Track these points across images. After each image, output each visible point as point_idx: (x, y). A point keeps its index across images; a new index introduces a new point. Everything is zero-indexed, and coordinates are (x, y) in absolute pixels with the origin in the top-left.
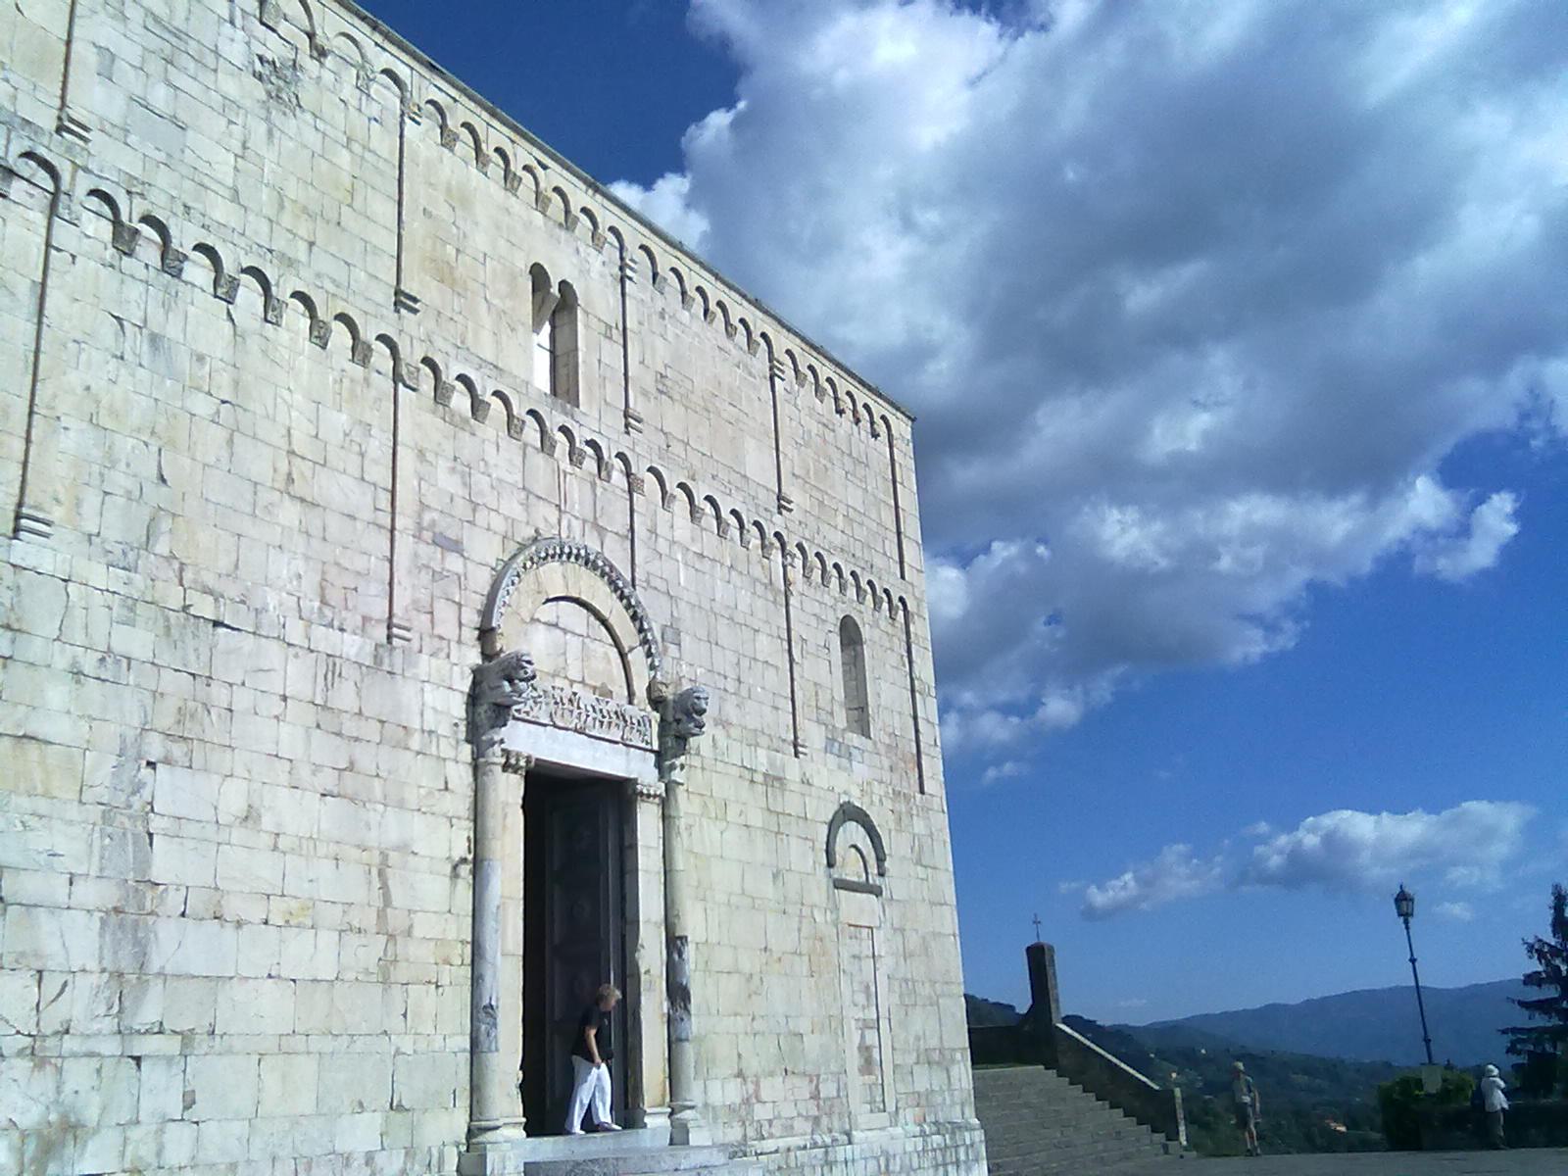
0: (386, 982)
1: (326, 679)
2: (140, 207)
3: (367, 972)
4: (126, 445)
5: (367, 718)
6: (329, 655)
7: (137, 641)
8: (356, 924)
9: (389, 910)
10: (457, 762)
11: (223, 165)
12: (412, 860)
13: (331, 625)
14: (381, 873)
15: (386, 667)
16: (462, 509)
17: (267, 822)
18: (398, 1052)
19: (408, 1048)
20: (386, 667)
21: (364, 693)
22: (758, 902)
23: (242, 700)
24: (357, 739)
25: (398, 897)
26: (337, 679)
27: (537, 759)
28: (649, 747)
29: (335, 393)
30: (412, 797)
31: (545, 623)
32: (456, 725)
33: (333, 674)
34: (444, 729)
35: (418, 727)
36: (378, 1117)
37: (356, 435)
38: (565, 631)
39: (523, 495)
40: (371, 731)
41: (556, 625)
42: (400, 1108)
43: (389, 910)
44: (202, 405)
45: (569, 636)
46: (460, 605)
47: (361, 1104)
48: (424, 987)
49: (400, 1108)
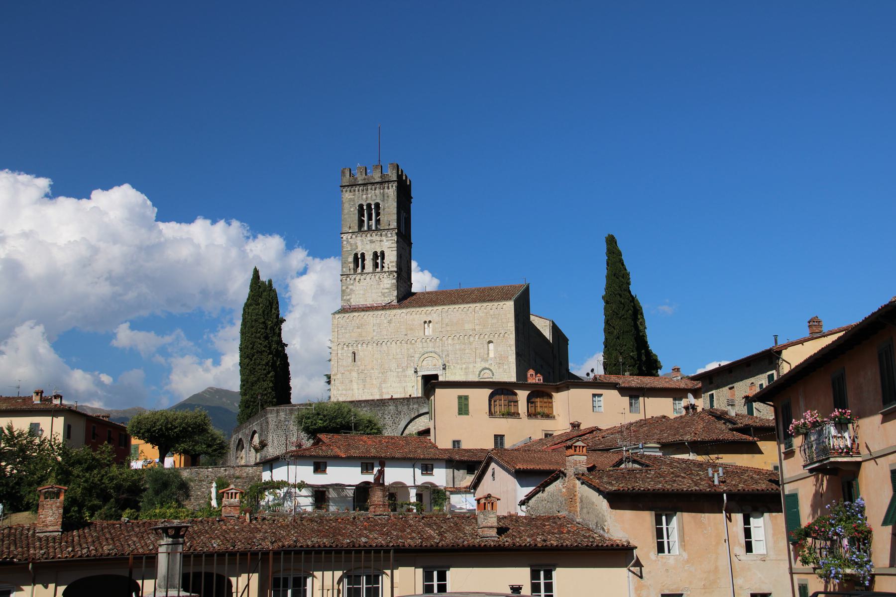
4: (379, 361)
7: (380, 375)
11: (385, 333)
23: (389, 377)
25: (406, 390)
44: (385, 355)
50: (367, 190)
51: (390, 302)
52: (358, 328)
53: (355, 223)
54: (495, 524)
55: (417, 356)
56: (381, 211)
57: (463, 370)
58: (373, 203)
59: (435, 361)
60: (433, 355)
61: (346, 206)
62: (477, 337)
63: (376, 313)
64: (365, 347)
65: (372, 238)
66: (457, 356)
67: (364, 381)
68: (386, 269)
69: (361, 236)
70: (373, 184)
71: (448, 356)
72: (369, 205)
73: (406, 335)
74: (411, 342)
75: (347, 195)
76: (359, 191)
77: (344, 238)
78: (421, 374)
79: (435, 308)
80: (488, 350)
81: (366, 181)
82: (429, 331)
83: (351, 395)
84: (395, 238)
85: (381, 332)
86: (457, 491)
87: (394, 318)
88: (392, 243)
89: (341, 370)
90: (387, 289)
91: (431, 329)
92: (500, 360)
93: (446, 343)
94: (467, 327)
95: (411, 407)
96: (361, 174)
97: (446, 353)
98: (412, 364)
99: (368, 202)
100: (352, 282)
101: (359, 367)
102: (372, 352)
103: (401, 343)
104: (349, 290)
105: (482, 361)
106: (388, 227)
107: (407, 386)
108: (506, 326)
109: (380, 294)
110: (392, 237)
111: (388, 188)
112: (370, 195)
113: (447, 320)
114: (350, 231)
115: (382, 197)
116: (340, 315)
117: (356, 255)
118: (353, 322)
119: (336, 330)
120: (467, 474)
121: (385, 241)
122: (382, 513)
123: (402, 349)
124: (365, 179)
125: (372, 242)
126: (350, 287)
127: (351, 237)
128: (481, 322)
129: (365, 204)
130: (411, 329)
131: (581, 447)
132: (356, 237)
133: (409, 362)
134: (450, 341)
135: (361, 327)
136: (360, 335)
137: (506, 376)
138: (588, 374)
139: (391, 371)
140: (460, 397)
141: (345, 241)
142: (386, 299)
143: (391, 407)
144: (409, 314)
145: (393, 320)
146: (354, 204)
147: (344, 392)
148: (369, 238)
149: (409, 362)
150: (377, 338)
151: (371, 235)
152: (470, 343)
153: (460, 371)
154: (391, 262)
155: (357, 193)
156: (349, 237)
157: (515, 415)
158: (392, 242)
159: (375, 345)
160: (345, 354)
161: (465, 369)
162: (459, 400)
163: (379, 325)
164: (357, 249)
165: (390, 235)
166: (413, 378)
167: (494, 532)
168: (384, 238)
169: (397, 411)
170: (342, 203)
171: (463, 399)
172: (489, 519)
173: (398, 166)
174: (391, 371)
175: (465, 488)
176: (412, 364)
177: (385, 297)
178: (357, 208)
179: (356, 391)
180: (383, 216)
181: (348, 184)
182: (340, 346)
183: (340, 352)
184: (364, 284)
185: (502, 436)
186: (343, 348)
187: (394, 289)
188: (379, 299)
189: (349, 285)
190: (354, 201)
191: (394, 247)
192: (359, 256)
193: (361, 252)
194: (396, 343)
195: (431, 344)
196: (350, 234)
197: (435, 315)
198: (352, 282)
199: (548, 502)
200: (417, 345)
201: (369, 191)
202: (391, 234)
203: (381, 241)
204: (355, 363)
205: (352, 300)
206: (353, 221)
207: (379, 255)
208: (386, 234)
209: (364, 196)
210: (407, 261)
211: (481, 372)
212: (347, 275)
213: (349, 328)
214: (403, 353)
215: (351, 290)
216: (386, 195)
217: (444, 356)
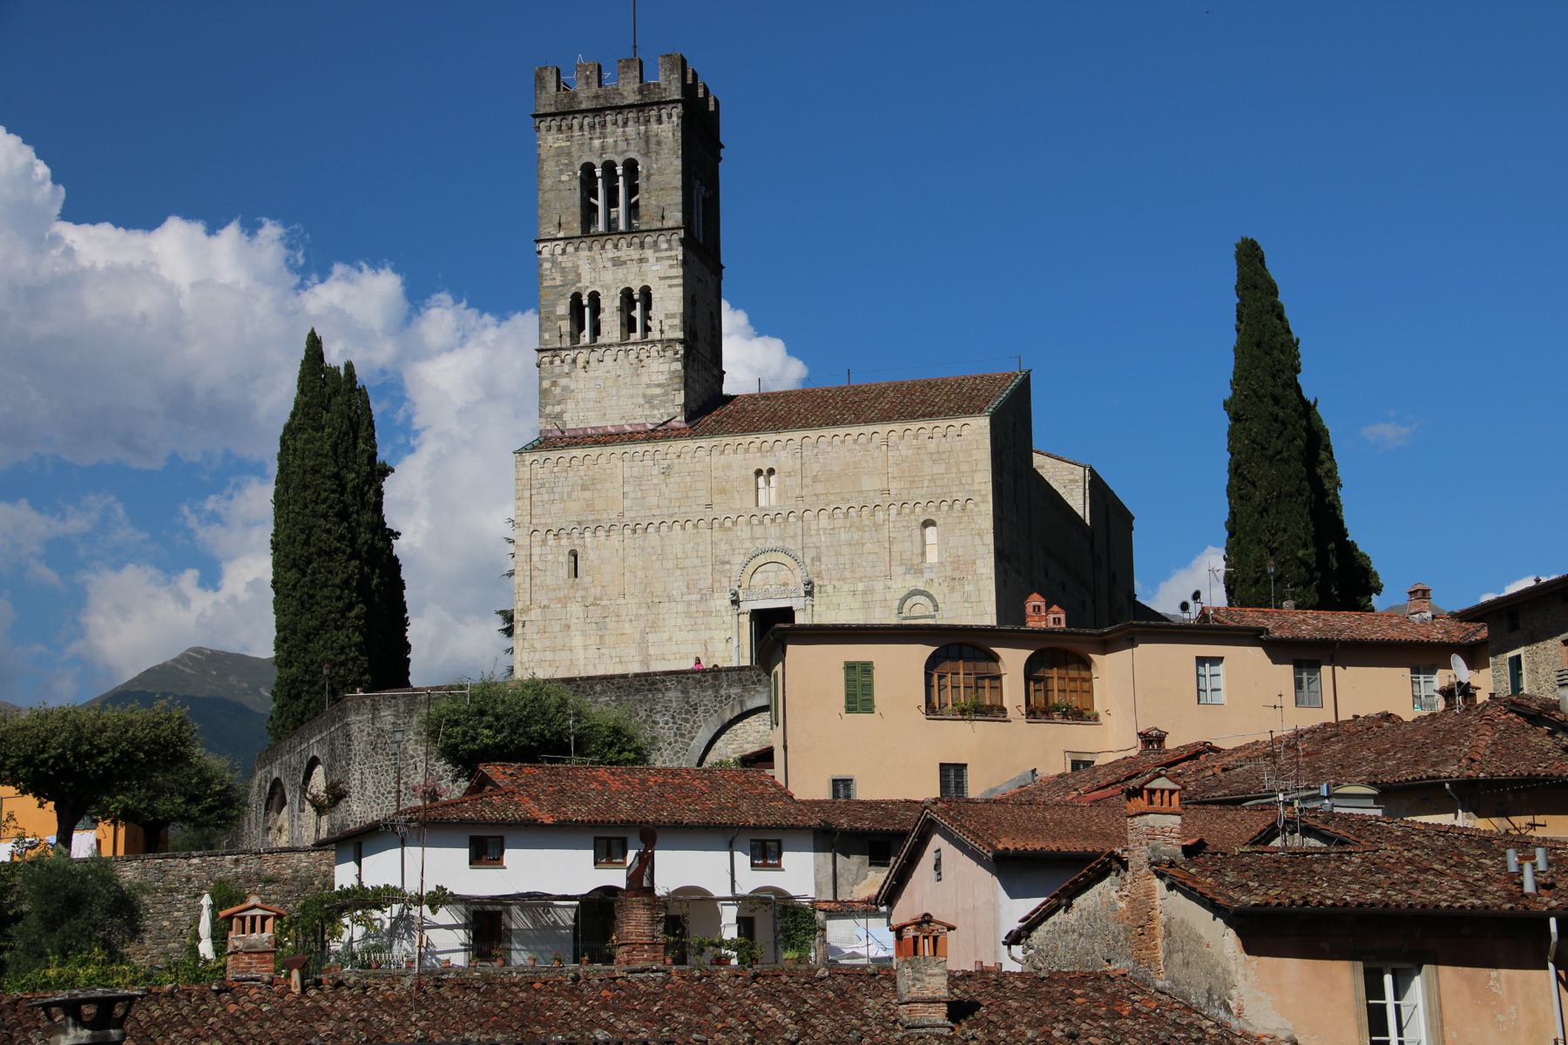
2: (635, 523)
4: (639, 574)
11: (655, 501)
17: (674, 639)
34: (723, 609)
44: (654, 558)
50: (604, 126)
51: (665, 419)
52: (584, 488)
53: (573, 213)
54: (943, 993)
55: (738, 560)
56: (641, 182)
57: (859, 598)
58: (619, 160)
59: (784, 574)
60: (781, 557)
61: (549, 167)
62: (893, 510)
63: (630, 448)
64: (603, 538)
65: (618, 254)
66: (841, 560)
67: (601, 625)
68: (654, 335)
69: (590, 249)
70: (619, 109)
71: (819, 560)
72: (609, 167)
73: (709, 506)
74: (721, 525)
75: (551, 140)
76: (581, 128)
77: (546, 253)
78: (747, 606)
79: (784, 436)
80: (924, 544)
81: (602, 102)
82: (769, 495)
83: (568, 663)
84: (679, 252)
85: (644, 498)
86: (844, 910)
87: (677, 461)
88: (671, 266)
89: (542, 597)
90: (659, 385)
91: (773, 492)
92: (953, 570)
93: (814, 526)
94: (870, 484)
95: (723, 692)
96: (587, 84)
97: (812, 553)
98: (725, 582)
99: (607, 157)
100: (566, 368)
101: (586, 589)
102: (621, 551)
103: (695, 526)
104: (558, 390)
105: (907, 572)
106: (659, 225)
107: (712, 638)
108: (969, 481)
109: (641, 401)
110: (670, 249)
111: (660, 121)
112: (610, 140)
113: (816, 467)
114: (561, 235)
115: (642, 144)
116: (536, 456)
117: (576, 297)
118: (571, 474)
119: (527, 494)
120: (871, 864)
121: (652, 260)
122: (648, 964)
123: (698, 544)
124: (597, 97)
125: (617, 263)
126: (563, 381)
127: (564, 251)
128: (904, 472)
129: (598, 162)
130: (723, 491)
131: (1167, 793)
132: (577, 249)
133: (717, 576)
134: (824, 521)
135: (591, 487)
136: (587, 506)
137: (970, 612)
138: (1184, 607)
139: (670, 599)
140: (850, 667)
141: (546, 260)
142: (656, 412)
143: (671, 695)
144: (715, 453)
145: (676, 468)
146: (571, 164)
147: (549, 656)
148: (610, 252)
149: (717, 576)
150: (633, 514)
151: (616, 246)
152: (877, 527)
153: (850, 599)
154: (668, 316)
155: (577, 133)
156: (558, 250)
157: (995, 712)
158: (671, 262)
159: (627, 532)
160: (550, 557)
161: (864, 593)
162: (847, 674)
163: (639, 480)
164: (580, 282)
165: (664, 246)
166: (728, 619)
167: (939, 1015)
168: (649, 253)
169: (688, 702)
170: (538, 161)
171: (858, 669)
172: (927, 979)
173: (684, 62)
174: (670, 599)
175: (863, 902)
176: (725, 582)
177: (653, 407)
178: (579, 173)
179: (580, 653)
180: (646, 196)
181: (553, 110)
182: (538, 537)
183: (536, 551)
184: (600, 373)
185: (960, 768)
186: (544, 542)
187: (676, 386)
188: (639, 412)
189: (560, 375)
190: (569, 154)
191: (676, 277)
192: (585, 302)
193: (589, 290)
194: (683, 528)
195: (773, 530)
196: (561, 243)
197: (784, 454)
198: (566, 368)
199: (1081, 935)
200: (739, 533)
201: (610, 128)
202: (669, 241)
203: (641, 260)
204: (578, 580)
205: (566, 417)
206: (568, 209)
207: (636, 297)
208: (655, 243)
209: (597, 143)
210: (711, 313)
211: (903, 601)
212: (555, 350)
213: (559, 490)
214: (700, 554)
215: (565, 389)
216: (653, 140)
217: (808, 561)
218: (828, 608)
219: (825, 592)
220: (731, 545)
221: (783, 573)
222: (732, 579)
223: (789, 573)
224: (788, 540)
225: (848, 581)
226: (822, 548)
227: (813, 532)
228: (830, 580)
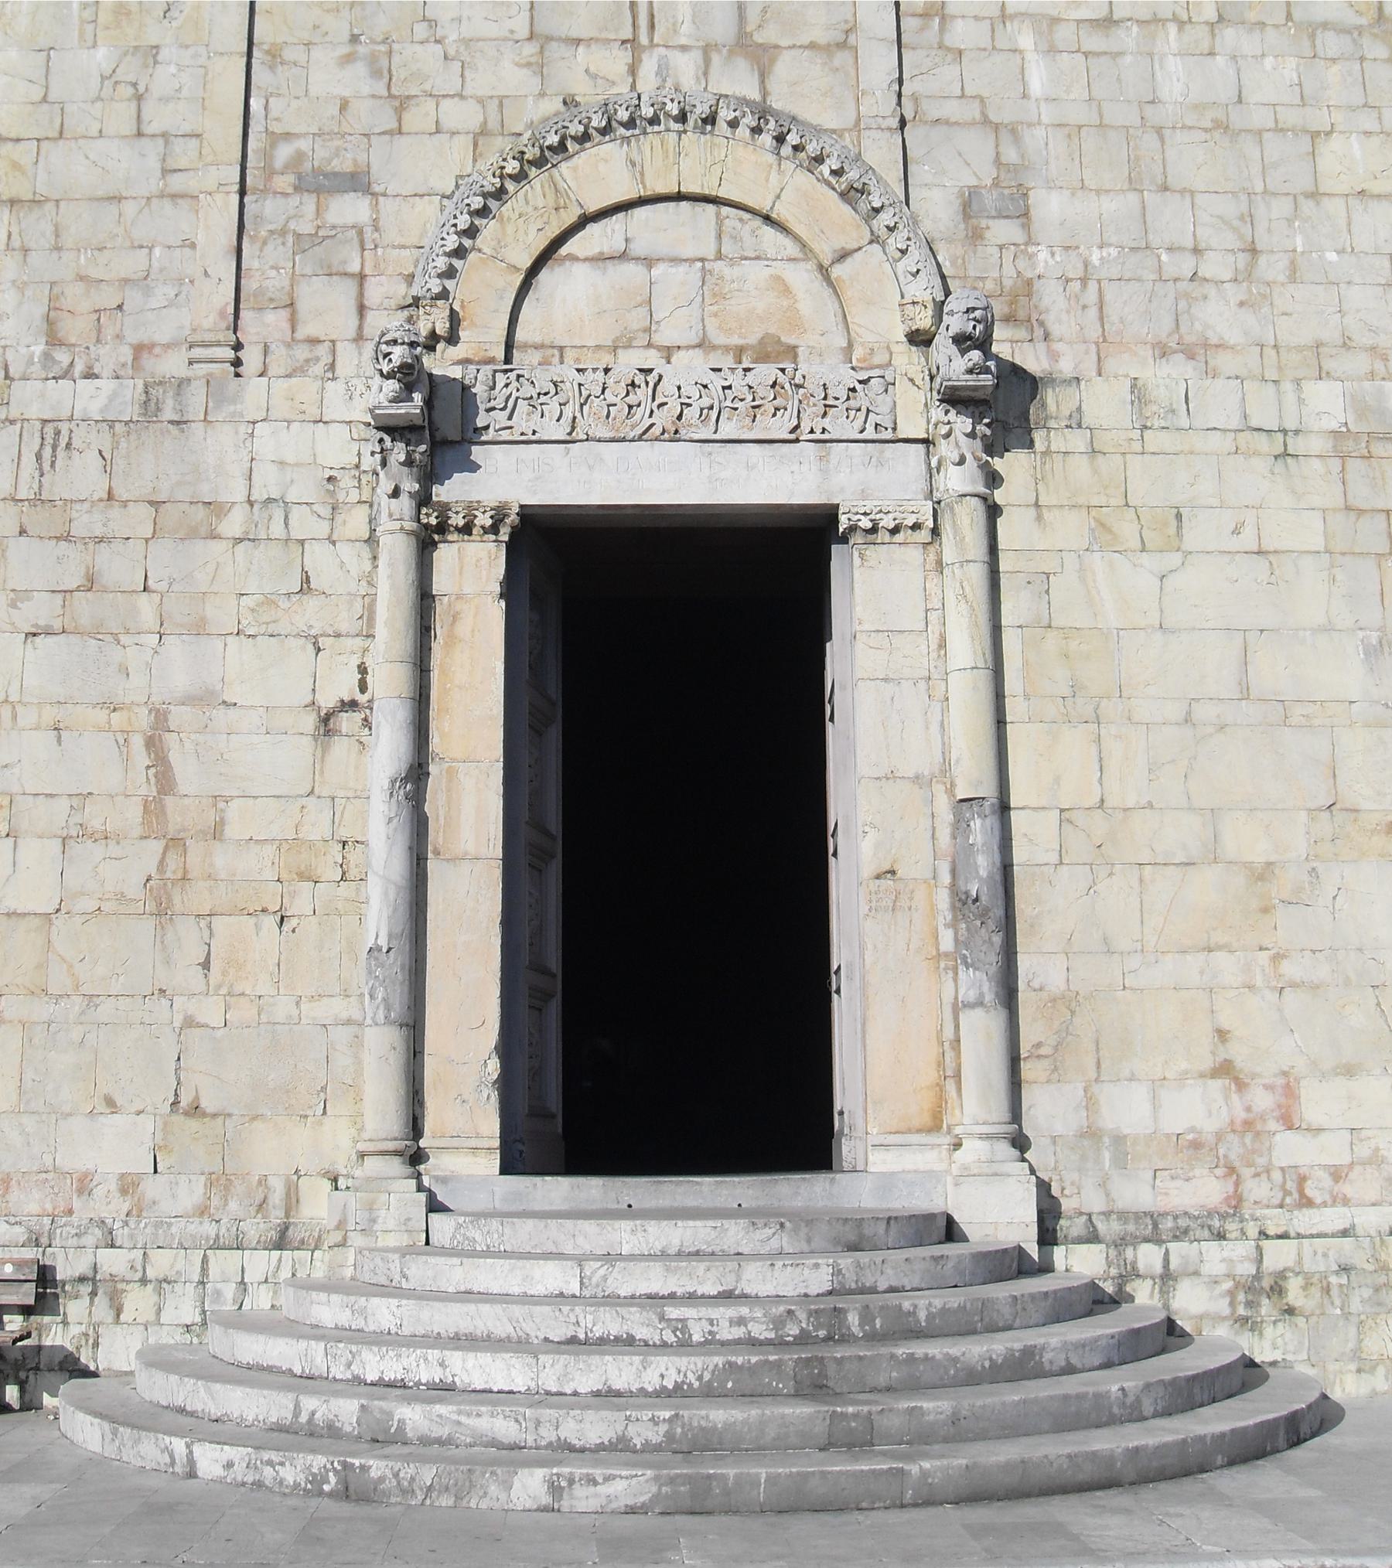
0: (163, 912)
1: (39, 457)
3: (121, 897)
5: (125, 504)
6: (45, 421)
8: (96, 824)
9: (169, 801)
10: (334, 543)
12: (220, 714)
13: (67, 374)
14: (152, 744)
15: (168, 414)
16: (371, 115)
18: (189, 1022)
19: (210, 1012)
20: (168, 414)
21: (120, 465)
22: (1298, 710)
24: (101, 540)
26: (61, 453)
27: (522, 507)
28: (888, 435)
29: (83, 22)
30: (222, 614)
31: (586, 259)
32: (330, 479)
33: (54, 448)
34: (304, 488)
35: (240, 496)
36: (147, 1123)
37: (129, 71)
38: (649, 262)
39: (530, 49)
40: (140, 520)
41: (623, 256)
42: (195, 1110)
43: (169, 801)
45: (658, 271)
46: (362, 277)
47: (110, 1102)
48: (252, 920)
49: (195, 1110)
107: (205, 699)
214: (158, 119)
218: (1102, 534)
219: (1076, 422)
220: (381, 70)
221: (757, 273)
222: (375, 292)
223: (802, 278)
224: (784, 69)
225: (1224, 362)
226: (1035, 138)
227: (961, 33)
228: (1103, 347)
